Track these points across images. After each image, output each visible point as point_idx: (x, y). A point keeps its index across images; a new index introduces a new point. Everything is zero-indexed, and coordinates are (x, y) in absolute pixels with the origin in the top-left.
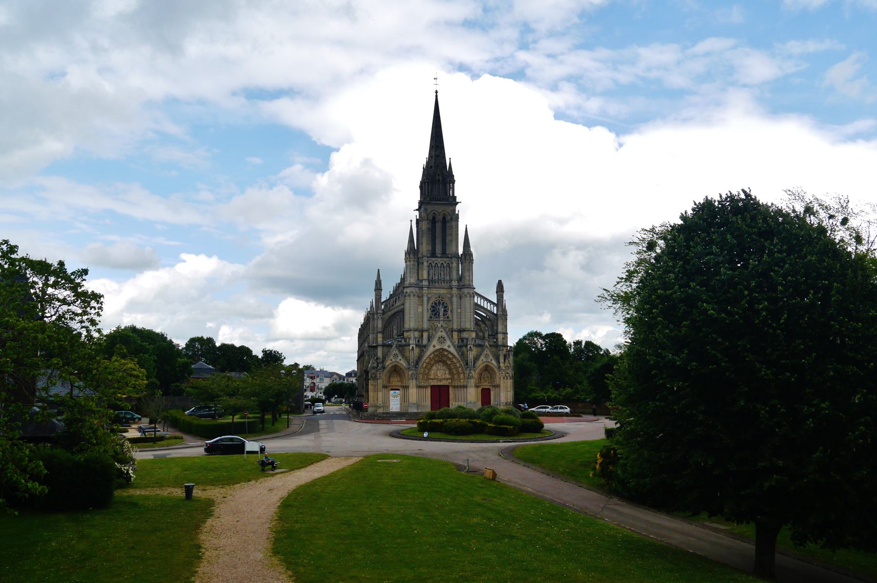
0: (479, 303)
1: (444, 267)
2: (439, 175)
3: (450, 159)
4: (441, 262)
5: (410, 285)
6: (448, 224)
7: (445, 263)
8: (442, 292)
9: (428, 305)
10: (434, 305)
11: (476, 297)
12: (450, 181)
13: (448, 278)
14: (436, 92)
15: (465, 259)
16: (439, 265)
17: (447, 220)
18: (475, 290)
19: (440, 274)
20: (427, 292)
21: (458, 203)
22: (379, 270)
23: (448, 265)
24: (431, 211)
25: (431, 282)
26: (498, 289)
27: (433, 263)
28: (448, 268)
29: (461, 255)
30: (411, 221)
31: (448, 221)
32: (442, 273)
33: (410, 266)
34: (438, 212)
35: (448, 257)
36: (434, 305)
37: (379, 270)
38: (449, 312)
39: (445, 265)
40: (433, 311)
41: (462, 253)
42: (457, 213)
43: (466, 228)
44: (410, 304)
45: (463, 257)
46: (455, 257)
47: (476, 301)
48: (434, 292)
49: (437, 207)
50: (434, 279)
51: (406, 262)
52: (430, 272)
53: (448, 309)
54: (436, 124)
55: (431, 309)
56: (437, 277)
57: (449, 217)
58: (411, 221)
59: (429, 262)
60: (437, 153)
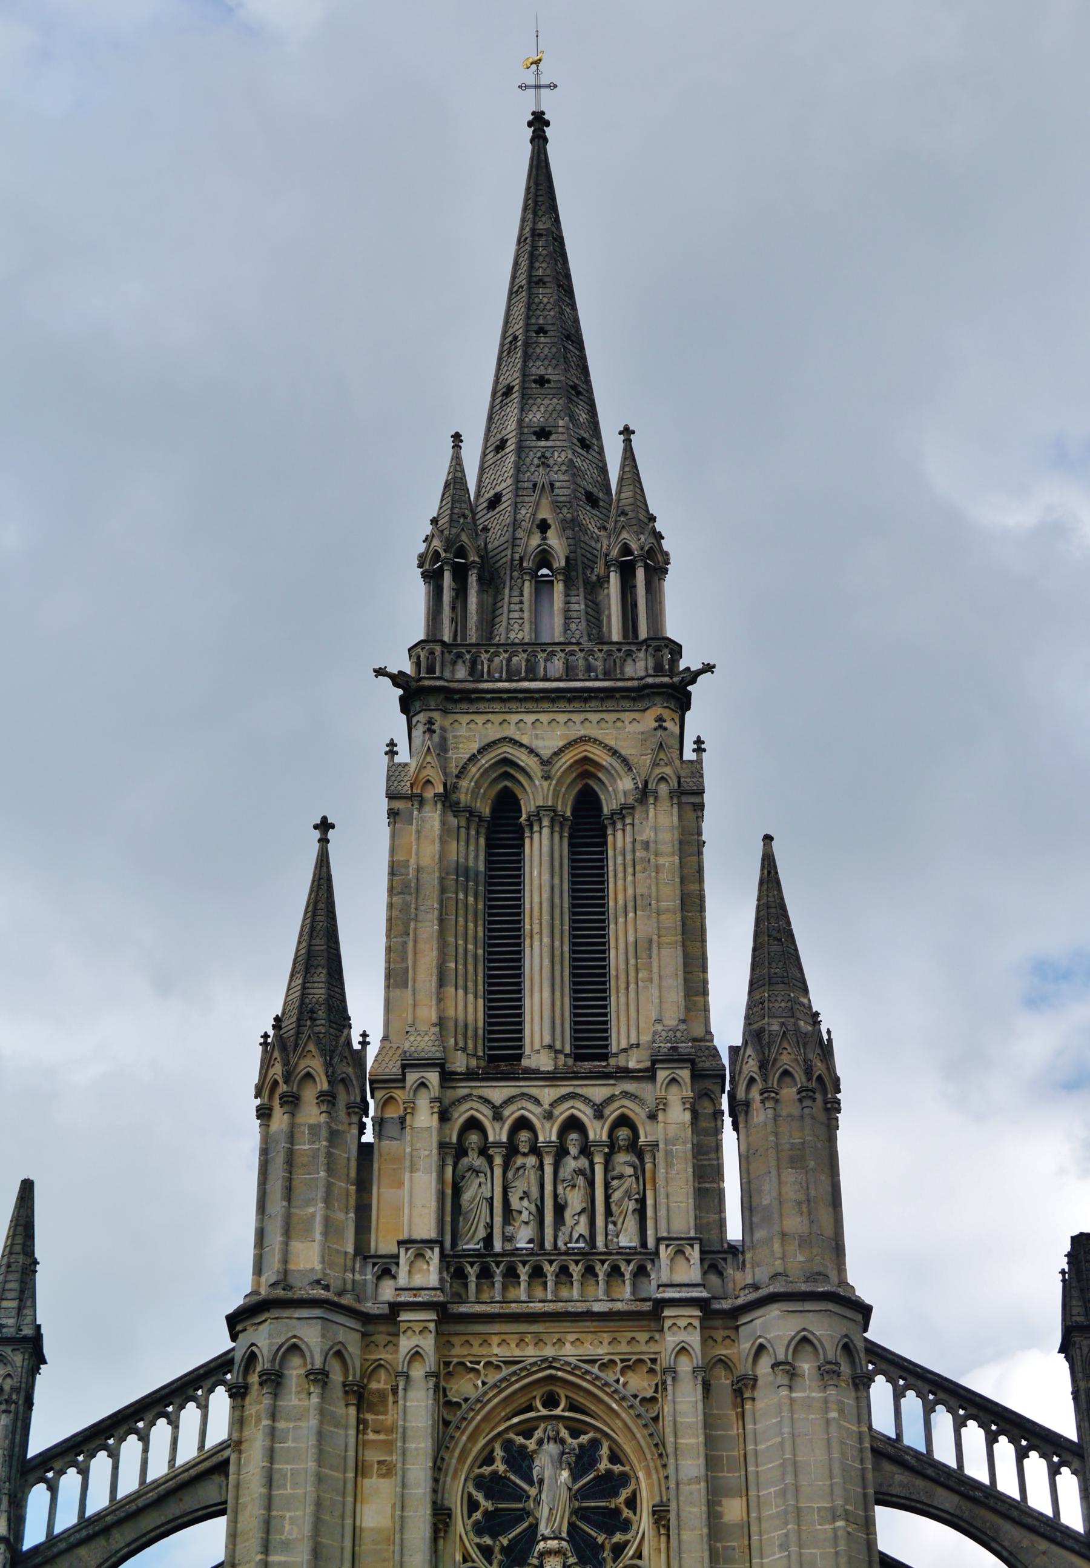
0: (913, 1439)
1: (586, 1151)
2: (544, 526)
3: (627, 432)
4: (563, 1112)
5: (280, 1293)
6: (618, 840)
7: (599, 1114)
8: (569, 1351)
9: (438, 1467)
10: (500, 1466)
11: (881, 1390)
12: (626, 550)
13: (627, 1239)
14: (539, 122)
15: (763, 1065)
16: (548, 1133)
17: (609, 805)
18: (873, 1334)
19: (560, 1209)
20: (428, 1343)
21: (693, 677)
22: (27, 1188)
23: (623, 1133)
24: (482, 750)
25: (472, 1272)
26: (1077, 1308)
27: (498, 1117)
28: (623, 1161)
29: (734, 1051)
30: (325, 826)
31: (623, 812)
32: (575, 1200)
33: (291, 1137)
34: (532, 751)
35: (625, 1074)
36: (500, 1466)
37: (27, 1188)
38: (644, 1522)
39: (597, 1131)
40: (491, 1525)
41: (738, 1042)
42: (689, 755)
43: (769, 863)
44: (271, 1455)
45: (751, 1066)
46: (674, 1058)
47: (883, 1422)
48: (497, 1351)
49: (530, 718)
50: (498, 1246)
51: (264, 1114)
52: (466, 1197)
53: (632, 1503)
54: (531, 267)
55: (473, 1506)
56: (523, 1237)
57: (625, 784)
58: (325, 826)
59: (460, 1116)
60: (536, 417)
